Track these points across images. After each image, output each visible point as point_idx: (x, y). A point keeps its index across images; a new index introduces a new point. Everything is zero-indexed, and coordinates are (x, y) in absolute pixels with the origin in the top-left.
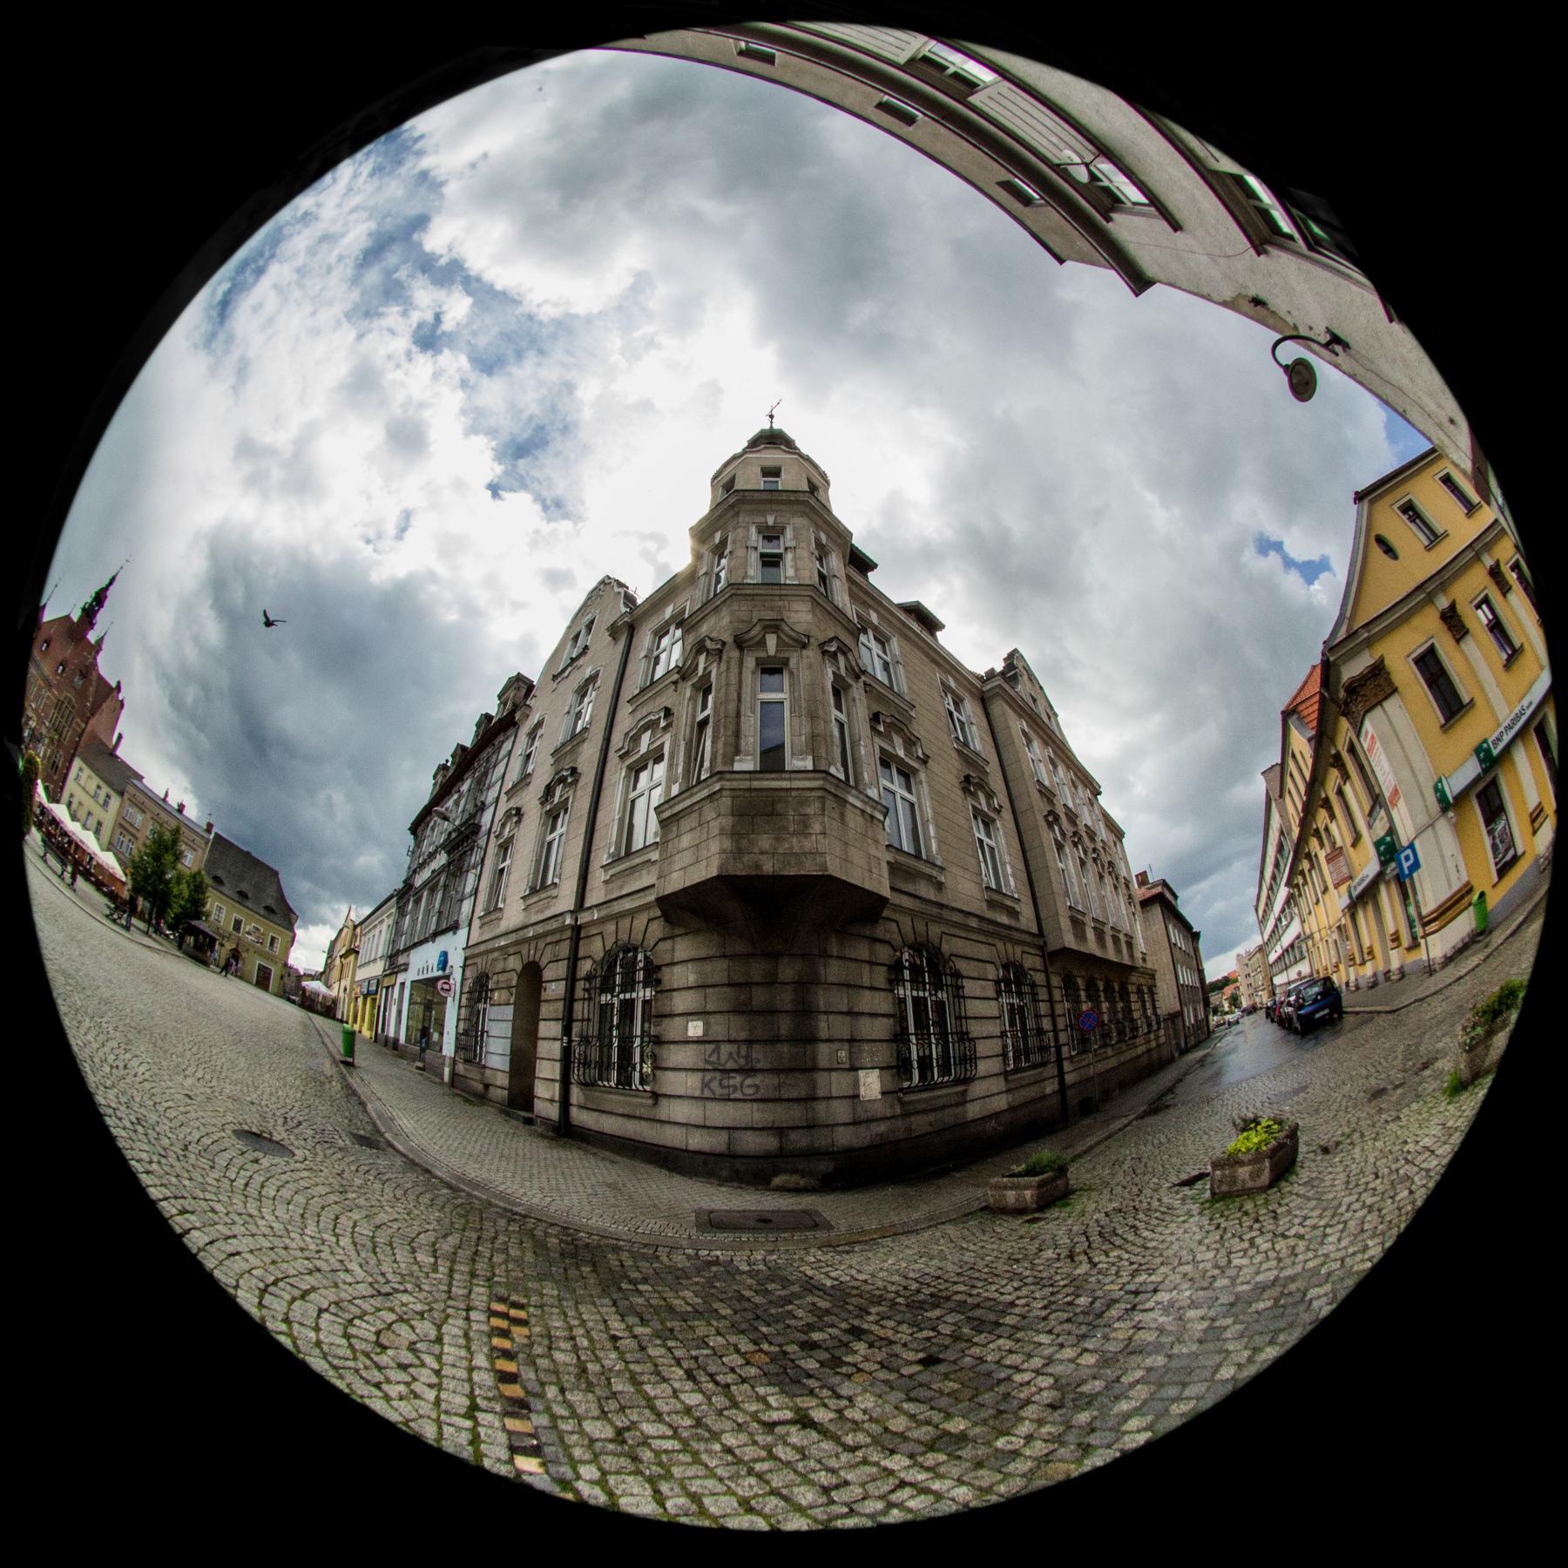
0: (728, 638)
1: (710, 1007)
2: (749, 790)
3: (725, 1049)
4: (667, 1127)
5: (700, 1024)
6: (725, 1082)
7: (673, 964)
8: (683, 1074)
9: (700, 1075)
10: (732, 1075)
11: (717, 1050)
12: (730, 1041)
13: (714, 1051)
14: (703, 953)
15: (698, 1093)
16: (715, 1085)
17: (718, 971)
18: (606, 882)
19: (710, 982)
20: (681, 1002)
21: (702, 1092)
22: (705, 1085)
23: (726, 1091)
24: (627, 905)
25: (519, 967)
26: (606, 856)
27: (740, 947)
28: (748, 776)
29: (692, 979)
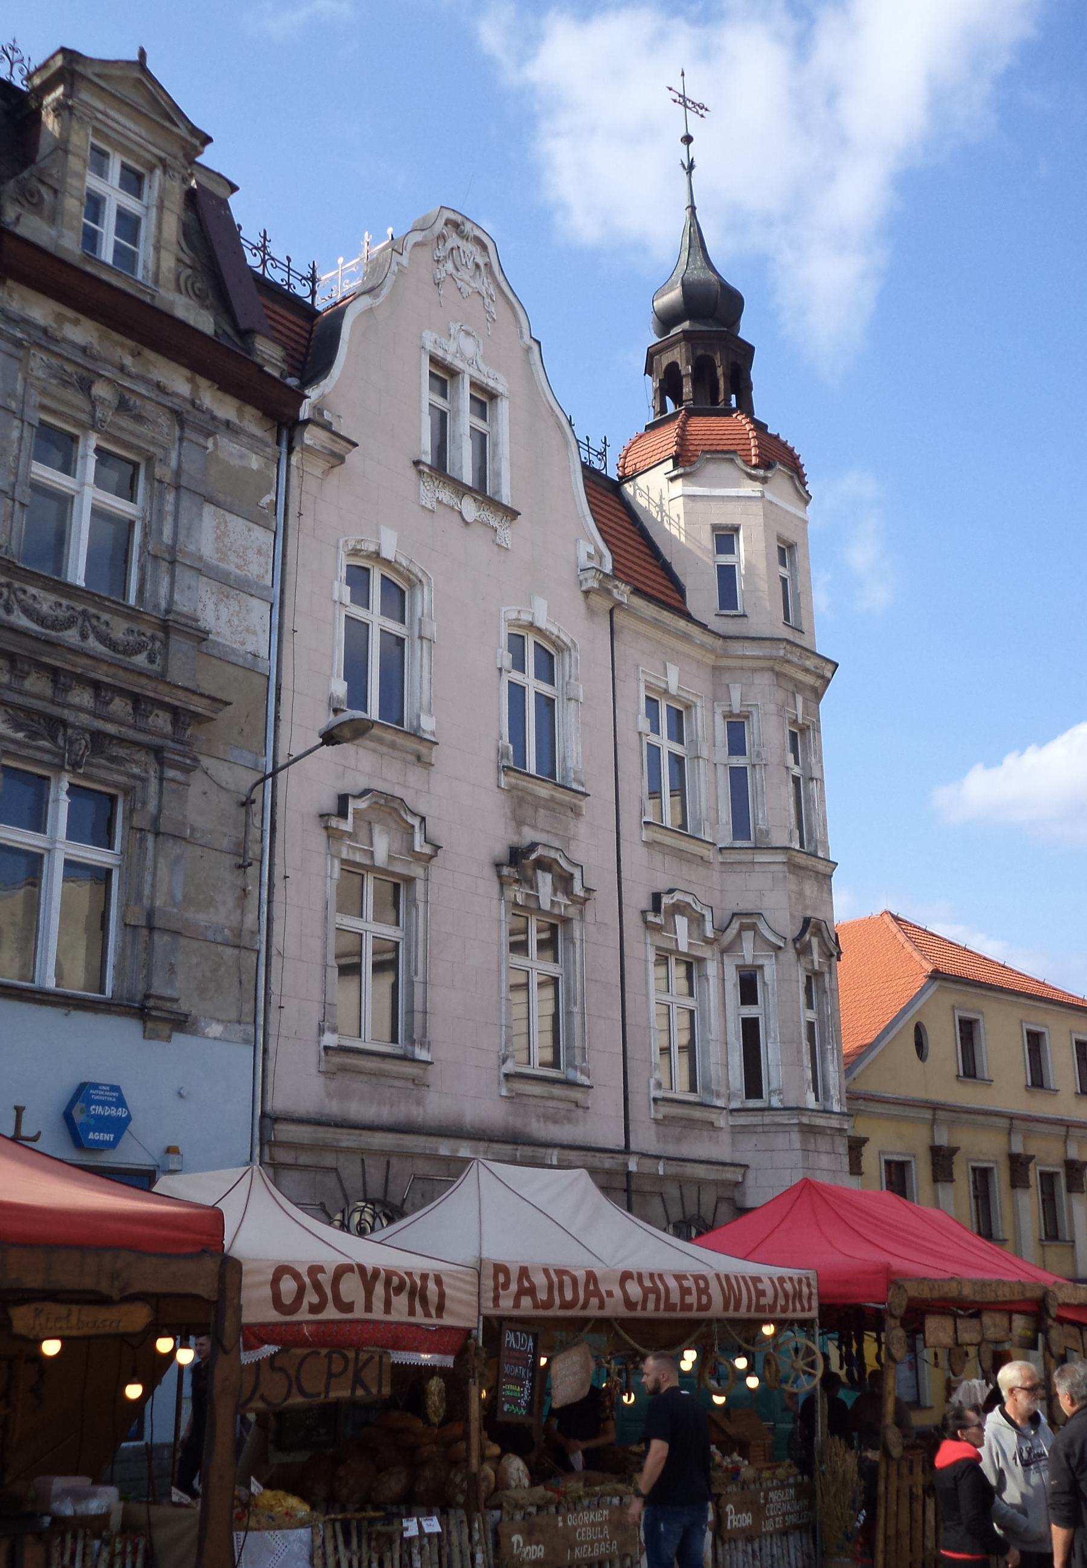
18: (656, 1121)
24: (701, 1171)
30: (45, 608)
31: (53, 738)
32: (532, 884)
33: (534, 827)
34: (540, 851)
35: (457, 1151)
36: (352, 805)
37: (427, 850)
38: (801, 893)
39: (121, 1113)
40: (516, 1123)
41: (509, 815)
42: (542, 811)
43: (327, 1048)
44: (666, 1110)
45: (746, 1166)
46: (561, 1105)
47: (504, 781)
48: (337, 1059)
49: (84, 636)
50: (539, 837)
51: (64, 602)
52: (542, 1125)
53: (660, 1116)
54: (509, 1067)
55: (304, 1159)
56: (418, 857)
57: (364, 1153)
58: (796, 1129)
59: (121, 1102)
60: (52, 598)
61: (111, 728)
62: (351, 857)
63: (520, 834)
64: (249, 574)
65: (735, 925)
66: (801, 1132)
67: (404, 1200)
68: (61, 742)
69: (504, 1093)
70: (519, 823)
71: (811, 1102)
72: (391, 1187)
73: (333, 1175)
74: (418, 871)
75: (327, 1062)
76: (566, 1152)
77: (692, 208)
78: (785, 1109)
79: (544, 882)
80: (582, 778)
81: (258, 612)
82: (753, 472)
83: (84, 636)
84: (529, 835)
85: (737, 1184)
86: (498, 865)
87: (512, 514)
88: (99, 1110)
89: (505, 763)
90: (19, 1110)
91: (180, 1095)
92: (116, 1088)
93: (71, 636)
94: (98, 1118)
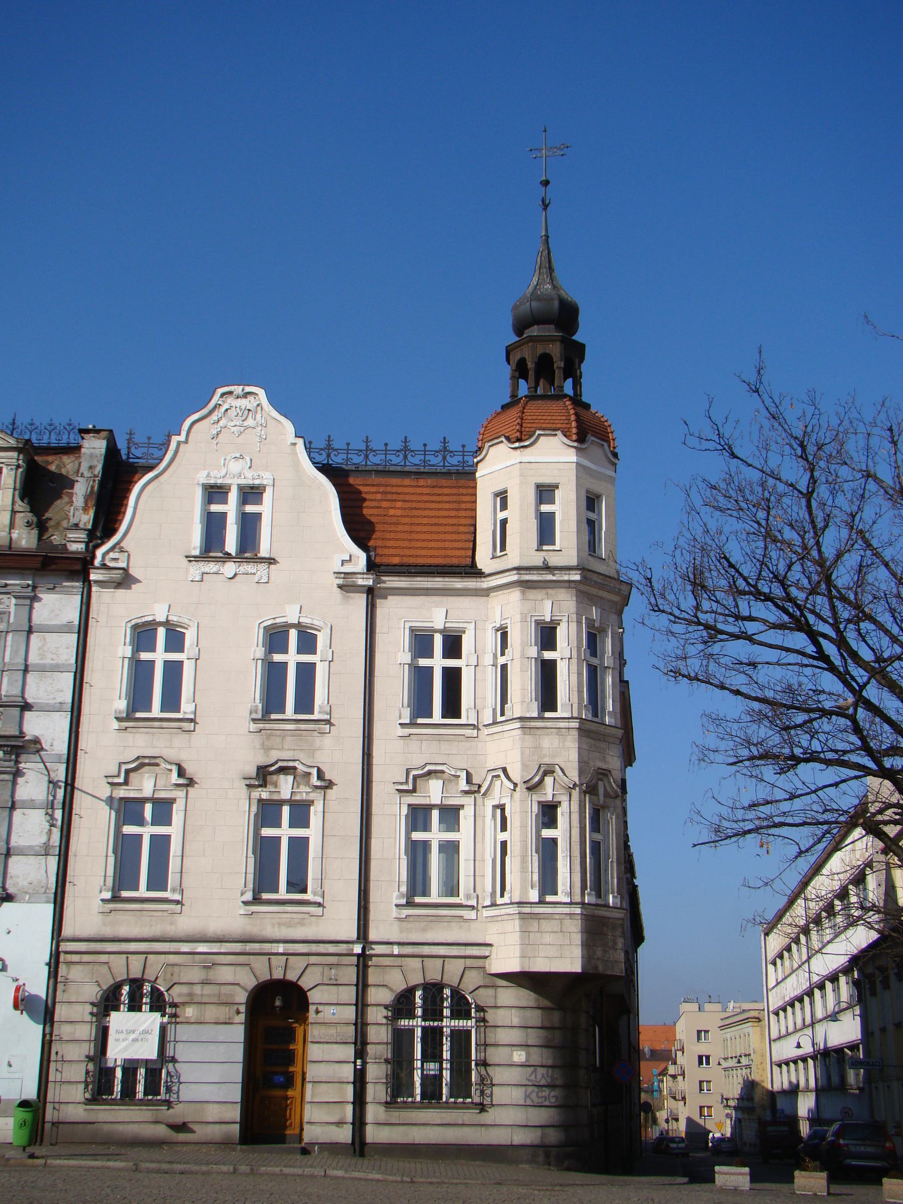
1: (530, 1042)
3: (541, 1071)
4: (491, 1129)
5: (523, 1053)
6: (540, 1094)
7: (496, 1007)
8: (508, 1089)
9: (523, 1089)
10: (544, 1089)
11: (535, 1070)
12: (542, 1066)
13: (533, 1072)
14: (524, 1003)
15: (522, 1102)
16: (534, 1096)
17: (535, 1017)
18: (399, 919)
19: (530, 1024)
20: (503, 1036)
21: (525, 1102)
22: (527, 1096)
23: (540, 1100)
24: (442, 951)
27: (546, 1003)
28: (594, 907)
29: (516, 1021)
33: (282, 749)
34: (280, 764)
35: (196, 949)
37: (181, 781)
38: (537, 748)
41: (258, 746)
42: (289, 739)
43: (103, 900)
46: (294, 916)
47: (253, 727)
48: (111, 906)
52: (276, 929)
58: (517, 916)
62: (127, 795)
63: (268, 756)
64: (60, 662)
65: (489, 778)
66: (521, 919)
67: (157, 978)
69: (242, 912)
70: (267, 749)
73: (106, 967)
75: (103, 907)
76: (286, 945)
78: (512, 903)
79: (286, 781)
81: (68, 679)
82: (513, 446)
84: (274, 755)
85: (486, 957)
87: (271, 561)
89: (254, 716)
91: (9, 932)
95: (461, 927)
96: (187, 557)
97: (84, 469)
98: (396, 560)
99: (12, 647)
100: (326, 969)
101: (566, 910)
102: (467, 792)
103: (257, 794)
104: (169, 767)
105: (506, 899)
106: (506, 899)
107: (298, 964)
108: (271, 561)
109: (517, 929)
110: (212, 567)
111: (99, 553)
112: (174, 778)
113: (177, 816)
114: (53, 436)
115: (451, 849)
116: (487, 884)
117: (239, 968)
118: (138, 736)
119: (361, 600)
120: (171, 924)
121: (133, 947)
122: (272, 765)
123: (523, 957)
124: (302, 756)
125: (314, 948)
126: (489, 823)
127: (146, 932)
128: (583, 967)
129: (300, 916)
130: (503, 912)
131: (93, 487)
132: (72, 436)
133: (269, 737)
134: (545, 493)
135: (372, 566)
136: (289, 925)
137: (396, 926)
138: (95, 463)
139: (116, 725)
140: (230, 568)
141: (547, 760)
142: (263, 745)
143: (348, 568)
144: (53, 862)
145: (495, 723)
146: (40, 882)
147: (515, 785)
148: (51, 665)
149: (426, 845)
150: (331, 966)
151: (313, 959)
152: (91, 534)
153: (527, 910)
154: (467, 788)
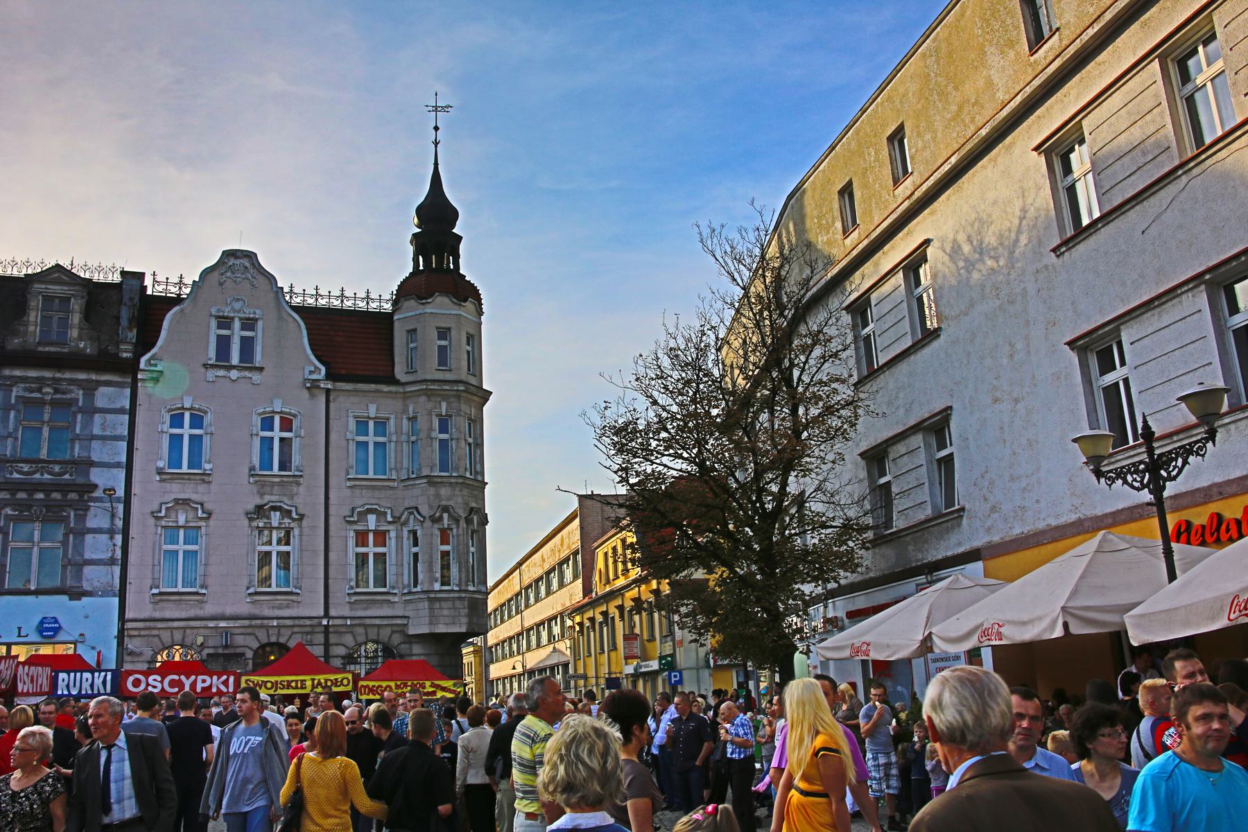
0: (464, 515)
2: (472, 598)
18: (349, 603)
24: (377, 622)
25: (255, 645)
26: (347, 587)
30: (26, 469)
31: (29, 511)
32: (269, 518)
33: (272, 494)
34: (271, 504)
36: (164, 507)
37: (205, 515)
38: (438, 496)
39: (57, 625)
40: (257, 612)
42: (276, 487)
43: (153, 594)
44: (354, 598)
45: (408, 617)
47: (252, 480)
48: (159, 598)
49: (42, 475)
50: (274, 498)
51: (34, 466)
53: (353, 600)
54: (252, 590)
55: (143, 633)
56: (201, 519)
57: (172, 629)
59: (56, 621)
60: (30, 465)
61: (51, 503)
65: (406, 513)
66: (428, 601)
68: (33, 511)
71: (437, 586)
72: (186, 640)
74: (203, 524)
77: (436, 164)
79: (275, 515)
80: (301, 468)
83: (42, 475)
84: (267, 498)
86: (247, 514)
87: (261, 369)
88: (47, 625)
90: (20, 629)
92: (54, 618)
93: (37, 476)
94: (47, 627)
95: (389, 607)
96: (204, 365)
97: (126, 299)
98: (344, 372)
99: (81, 423)
100: (304, 635)
101: (456, 595)
102: (390, 523)
103: (254, 524)
104: (195, 506)
105: (419, 589)
106: (419, 589)
107: (287, 632)
108: (261, 369)
109: (427, 606)
110: (222, 373)
111: (143, 360)
112: (200, 513)
113: (203, 541)
114: (101, 275)
115: (380, 558)
116: (406, 578)
117: (247, 637)
118: (173, 485)
119: (322, 399)
120: (201, 609)
121: (176, 624)
122: (266, 505)
123: (431, 624)
124: (285, 499)
125: (297, 622)
126: (407, 542)
127: (184, 615)
128: (467, 629)
129: (286, 602)
130: (416, 597)
131: (133, 313)
132: (115, 275)
133: (263, 486)
134: (443, 333)
135: (330, 376)
136: (280, 607)
137: (347, 607)
138: (133, 296)
139: (158, 478)
140: (234, 374)
141: (444, 503)
142: (258, 492)
143: (314, 377)
144: (117, 570)
145: (409, 479)
146: (108, 583)
147: (424, 518)
148: (111, 436)
149: (366, 555)
150: (307, 633)
151: (296, 630)
152: (136, 345)
153: (433, 596)
154: (391, 520)
